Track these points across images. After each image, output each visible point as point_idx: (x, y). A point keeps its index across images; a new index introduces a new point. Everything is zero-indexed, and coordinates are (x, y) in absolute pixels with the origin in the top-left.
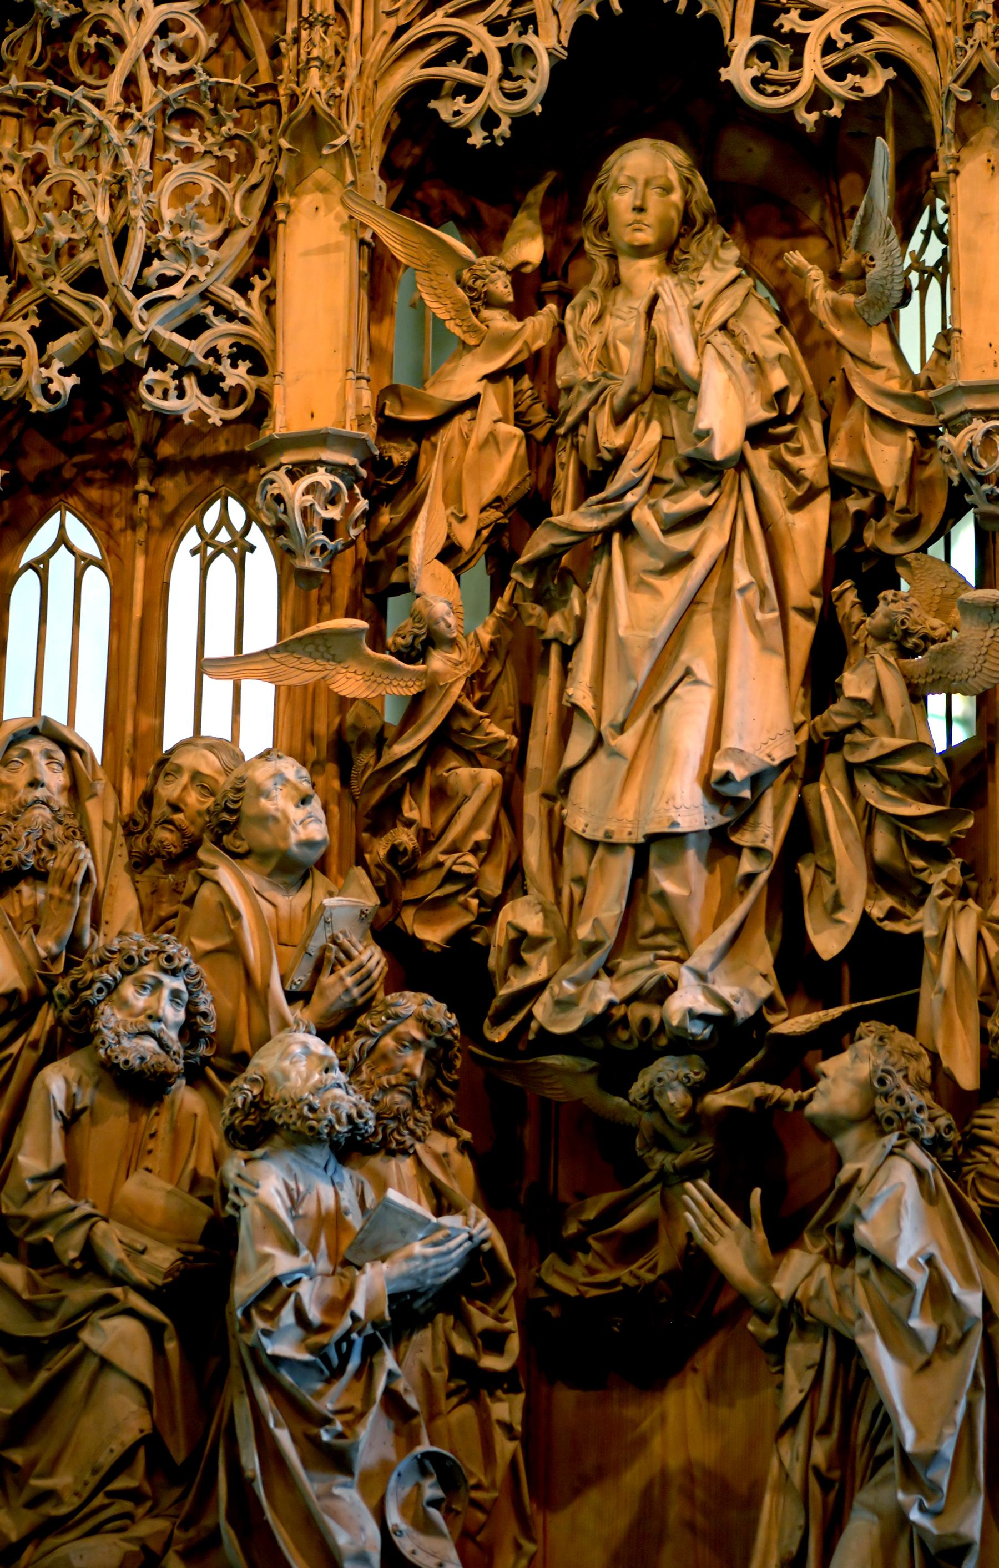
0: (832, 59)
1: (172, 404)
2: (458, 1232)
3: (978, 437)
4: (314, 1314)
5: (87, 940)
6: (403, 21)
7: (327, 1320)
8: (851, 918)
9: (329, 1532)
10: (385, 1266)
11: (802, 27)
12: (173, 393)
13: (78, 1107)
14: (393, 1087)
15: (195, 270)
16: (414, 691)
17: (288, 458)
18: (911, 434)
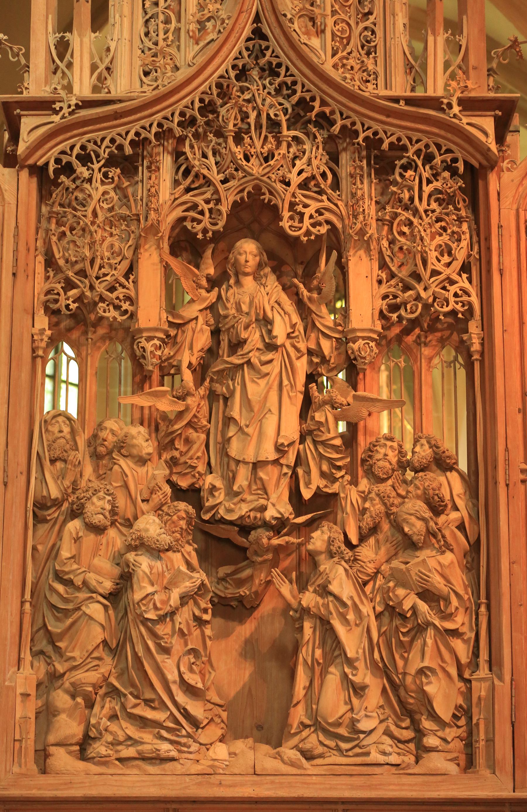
0: (312, 221)
1: (107, 314)
2: (198, 578)
3: (362, 346)
4: (159, 605)
5: (79, 482)
6: (177, 196)
11: (304, 210)
12: (107, 311)
13: (79, 536)
15: (114, 272)
16: (182, 409)
17: (145, 334)
18: (334, 340)
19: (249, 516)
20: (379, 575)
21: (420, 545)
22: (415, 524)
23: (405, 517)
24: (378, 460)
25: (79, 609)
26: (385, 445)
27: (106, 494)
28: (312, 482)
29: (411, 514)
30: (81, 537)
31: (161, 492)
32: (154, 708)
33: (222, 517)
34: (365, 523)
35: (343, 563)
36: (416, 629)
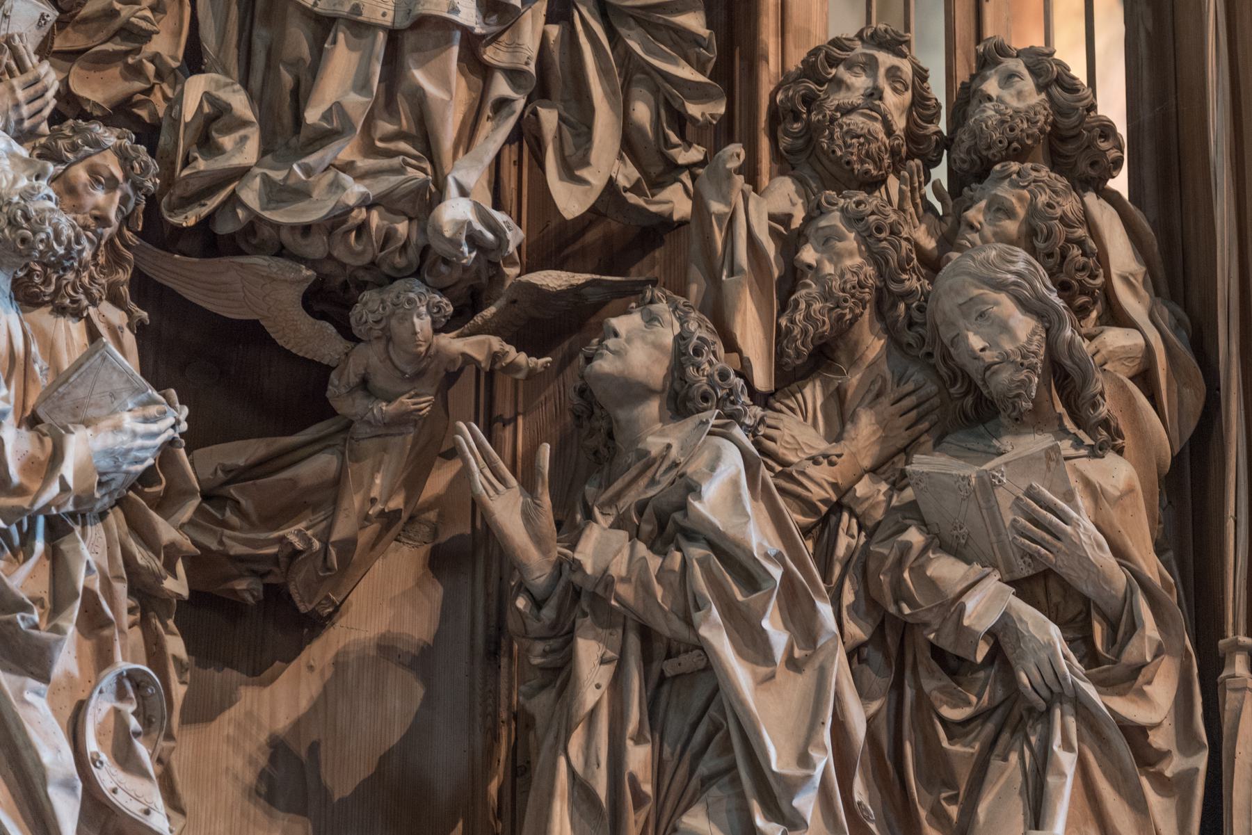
7: (26, 482)
8: (596, 177)
9: (29, 745)
10: (89, 432)
19: (362, 228)
20: (846, 516)
21: (1026, 405)
22: (1012, 323)
23: (976, 292)
24: (848, 110)
26: (870, 65)
28: (594, 156)
29: (1000, 286)
33: (255, 223)
34: (799, 317)
35: (738, 432)
36: (997, 717)
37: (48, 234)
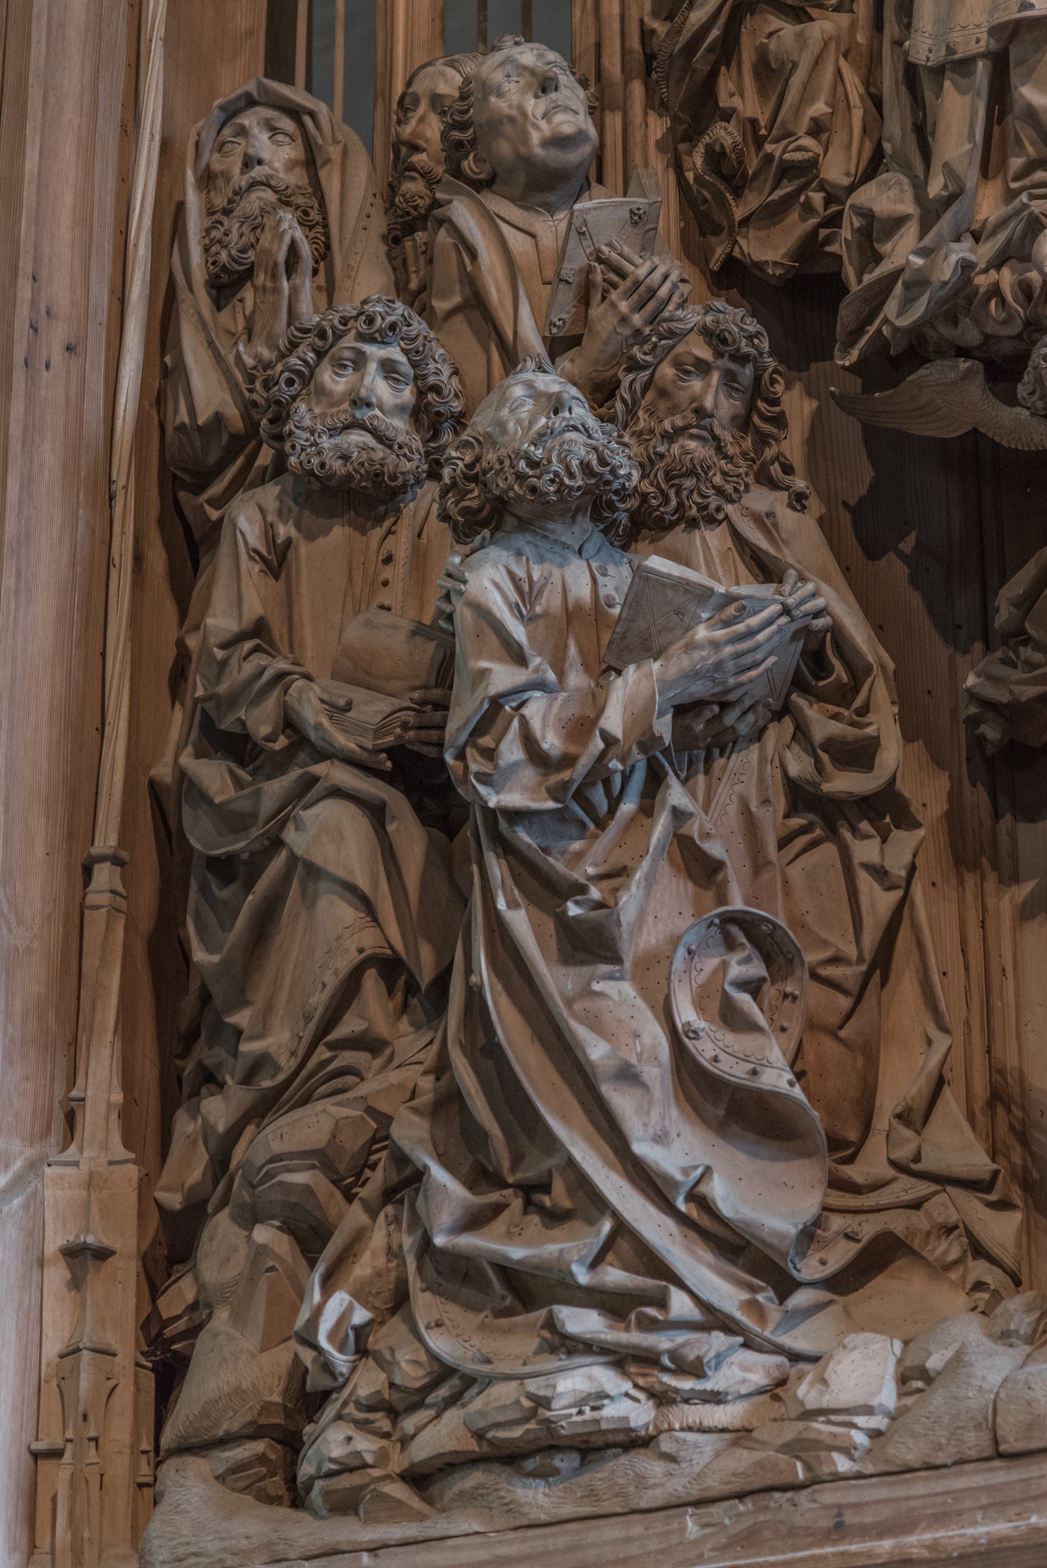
13: (279, 541)
14: (679, 432)
25: (277, 843)
27: (371, 339)
30: (288, 542)
31: (624, 285)
32: (555, 1218)
37: (556, 474)
